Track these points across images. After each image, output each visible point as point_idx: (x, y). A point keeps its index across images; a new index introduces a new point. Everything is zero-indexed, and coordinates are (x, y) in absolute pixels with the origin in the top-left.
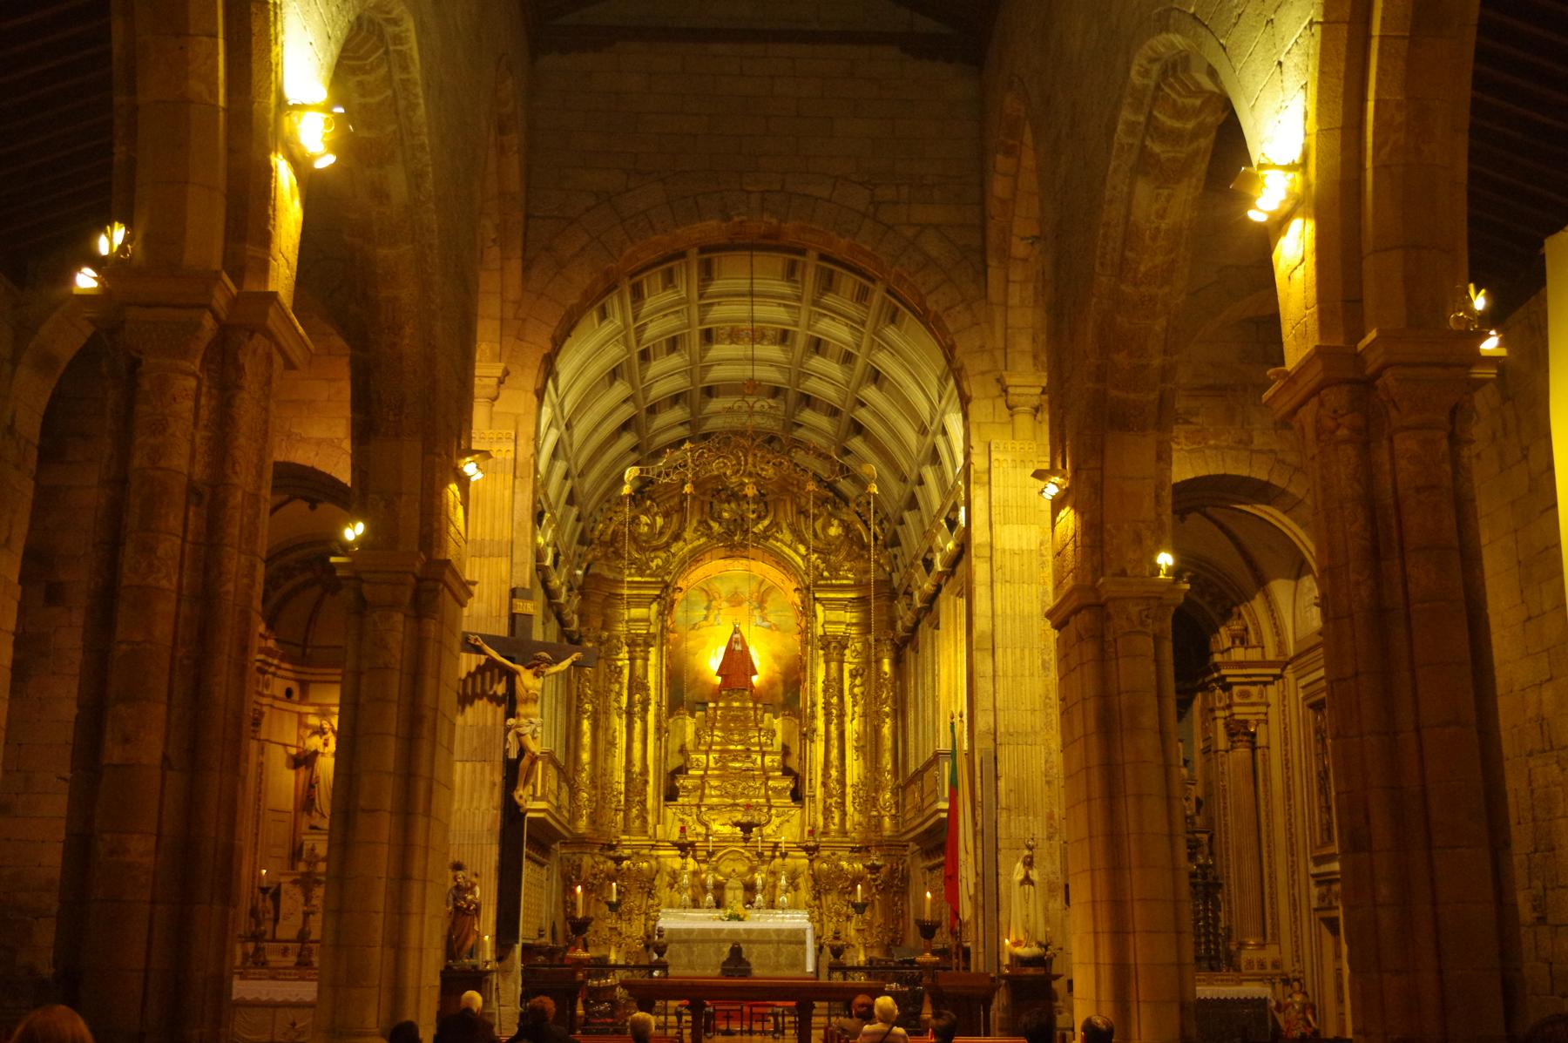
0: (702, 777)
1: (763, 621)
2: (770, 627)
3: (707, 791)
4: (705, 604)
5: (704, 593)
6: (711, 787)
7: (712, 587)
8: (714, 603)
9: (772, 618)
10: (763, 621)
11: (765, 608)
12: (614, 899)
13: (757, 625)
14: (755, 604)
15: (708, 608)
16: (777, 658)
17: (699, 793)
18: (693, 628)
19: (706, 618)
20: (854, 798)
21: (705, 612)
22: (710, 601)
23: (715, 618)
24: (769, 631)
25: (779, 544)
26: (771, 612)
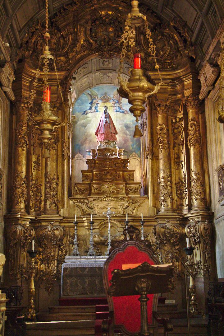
0: (89, 184)
2: (123, 112)
3: (93, 191)
4: (90, 101)
5: (89, 96)
6: (95, 189)
7: (93, 92)
8: (94, 101)
10: (120, 108)
11: (121, 103)
13: (117, 111)
15: (91, 103)
17: (88, 192)
18: (84, 114)
19: (90, 108)
20: (177, 191)
21: (90, 105)
22: (92, 100)
23: (96, 108)
24: (123, 114)
26: (124, 105)
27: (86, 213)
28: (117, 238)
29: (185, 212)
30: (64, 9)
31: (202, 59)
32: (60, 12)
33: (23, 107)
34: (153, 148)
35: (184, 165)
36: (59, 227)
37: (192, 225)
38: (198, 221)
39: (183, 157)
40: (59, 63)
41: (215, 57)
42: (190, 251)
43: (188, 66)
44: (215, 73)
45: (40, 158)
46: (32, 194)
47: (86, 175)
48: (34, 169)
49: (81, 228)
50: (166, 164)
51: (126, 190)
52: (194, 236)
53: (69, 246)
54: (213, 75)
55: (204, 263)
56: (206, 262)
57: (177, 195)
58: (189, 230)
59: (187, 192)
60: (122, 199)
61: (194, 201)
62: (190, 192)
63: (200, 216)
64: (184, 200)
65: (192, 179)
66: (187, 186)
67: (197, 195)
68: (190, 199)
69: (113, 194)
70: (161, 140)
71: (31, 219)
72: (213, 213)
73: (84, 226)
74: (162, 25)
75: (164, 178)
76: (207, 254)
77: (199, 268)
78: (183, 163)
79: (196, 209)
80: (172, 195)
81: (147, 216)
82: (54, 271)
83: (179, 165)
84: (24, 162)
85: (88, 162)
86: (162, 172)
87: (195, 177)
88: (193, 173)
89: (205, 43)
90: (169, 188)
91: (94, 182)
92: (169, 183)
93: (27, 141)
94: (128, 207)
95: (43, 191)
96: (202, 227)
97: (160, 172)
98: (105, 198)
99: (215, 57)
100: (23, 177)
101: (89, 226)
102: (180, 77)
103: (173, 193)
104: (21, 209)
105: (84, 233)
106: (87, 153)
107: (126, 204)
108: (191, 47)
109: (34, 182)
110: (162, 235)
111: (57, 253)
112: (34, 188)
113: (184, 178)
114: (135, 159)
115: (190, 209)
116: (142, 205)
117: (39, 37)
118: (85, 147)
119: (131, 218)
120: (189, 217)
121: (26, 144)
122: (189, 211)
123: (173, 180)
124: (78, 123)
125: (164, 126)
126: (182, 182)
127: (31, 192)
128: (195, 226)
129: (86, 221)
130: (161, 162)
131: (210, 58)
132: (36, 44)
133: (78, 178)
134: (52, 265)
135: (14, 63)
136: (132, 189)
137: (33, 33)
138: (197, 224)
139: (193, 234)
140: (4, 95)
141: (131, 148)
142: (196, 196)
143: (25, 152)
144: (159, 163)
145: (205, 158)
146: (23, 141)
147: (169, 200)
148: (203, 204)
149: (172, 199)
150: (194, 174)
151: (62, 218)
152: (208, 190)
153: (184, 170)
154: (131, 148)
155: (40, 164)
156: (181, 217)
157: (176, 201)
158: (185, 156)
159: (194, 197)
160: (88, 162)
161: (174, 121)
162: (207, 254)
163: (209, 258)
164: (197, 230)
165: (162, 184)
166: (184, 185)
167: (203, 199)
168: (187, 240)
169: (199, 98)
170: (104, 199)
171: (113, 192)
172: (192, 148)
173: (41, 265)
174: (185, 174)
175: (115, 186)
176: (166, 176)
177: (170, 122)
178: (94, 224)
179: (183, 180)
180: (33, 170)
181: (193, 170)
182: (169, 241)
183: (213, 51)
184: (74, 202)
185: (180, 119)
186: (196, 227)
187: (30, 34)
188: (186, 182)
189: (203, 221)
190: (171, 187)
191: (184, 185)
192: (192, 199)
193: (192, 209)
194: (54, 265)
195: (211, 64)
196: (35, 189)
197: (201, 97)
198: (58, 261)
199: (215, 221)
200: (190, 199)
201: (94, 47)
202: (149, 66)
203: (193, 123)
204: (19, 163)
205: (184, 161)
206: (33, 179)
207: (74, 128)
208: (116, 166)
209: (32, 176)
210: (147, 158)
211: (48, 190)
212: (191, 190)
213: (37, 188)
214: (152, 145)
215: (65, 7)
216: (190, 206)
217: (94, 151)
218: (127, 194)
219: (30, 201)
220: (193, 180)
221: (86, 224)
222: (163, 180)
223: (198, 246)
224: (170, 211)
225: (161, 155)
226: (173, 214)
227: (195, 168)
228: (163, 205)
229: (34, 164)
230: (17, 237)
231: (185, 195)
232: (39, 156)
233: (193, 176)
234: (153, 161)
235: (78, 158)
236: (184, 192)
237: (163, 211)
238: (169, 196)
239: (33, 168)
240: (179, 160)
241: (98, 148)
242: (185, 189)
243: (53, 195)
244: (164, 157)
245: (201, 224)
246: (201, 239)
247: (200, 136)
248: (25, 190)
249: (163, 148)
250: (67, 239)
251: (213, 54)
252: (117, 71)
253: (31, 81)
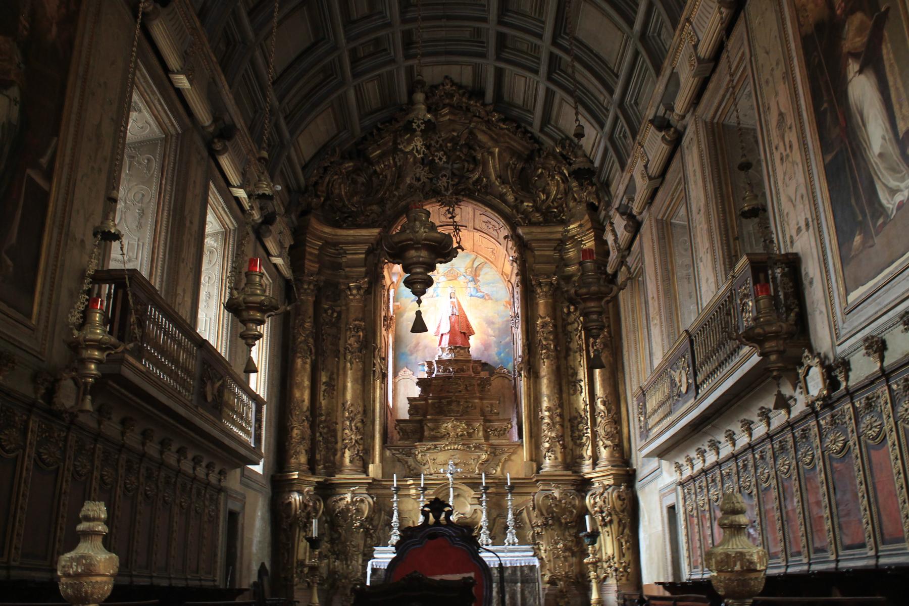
0: (420, 422)
1: (477, 291)
2: (483, 297)
3: (426, 433)
9: (485, 289)
10: (477, 290)
11: (479, 281)
12: (315, 534)
13: (471, 296)
14: (470, 278)
16: (490, 323)
24: (481, 300)
25: (488, 197)
27: (415, 471)
28: (468, 516)
29: (587, 469)
30: (379, 129)
31: (608, 205)
32: (371, 134)
33: (305, 290)
34: (529, 357)
35: (583, 387)
36: (366, 496)
37: (597, 493)
38: (608, 485)
39: (582, 373)
40: (369, 216)
41: (628, 203)
42: (594, 536)
43: (587, 217)
44: (629, 229)
45: (335, 376)
46: (321, 439)
47: (416, 405)
48: (324, 395)
49: (406, 499)
50: (552, 385)
51: (485, 431)
52: (602, 512)
53: (384, 530)
54: (625, 232)
55: (620, 559)
56: (624, 555)
57: (572, 440)
58: (592, 501)
59: (589, 435)
60: (478, 447)
61: (602, 449)
62: (595, 434)
63: (612, 476)
64: (585, 447)
66: (589, 424)
67: (607, 439)
68: (595, 446)
69: (462, 439)
70: (544, 343)
71: (317, 482)
72: (635, 471)
73: (409, 496)
74: (541, 152)
75: (549, 409)
76: (624, 543)
77: (611, 567)
78: (582, 384)
79: (606, 463)
80: (563, 440)
81: (520, 477)
82: (358, 572)
83: (575, 386)
84: (307, 383)
85: (421, 382)
86: (545, 399)
88: (599, 400)
89: (613, 180)
90: (558, 426)
91: (429, 417)
92: (558, 419)
93: (312, 347)
94: (487, 461)
95: (339, 434)
96: (615, 494)
97: (543, 400)
98: (447, 445)
99: (628, 203)
100: (305, 409)
101: (417, 495)
102: (574, 236)
103: (566, 436)
104: (300, 464)
105: (410, 507)
106: (420, 368)
107: (484, 457)
108: (590, 188)
109: (323, 418)
110: (547, 511)
111: (362, 543)
112: (324, 428)
113: (585, 410)
114: (503, 377)
115: (595, 464)
116: (513, 457)
117: (336, 174)
118: (416, 358)
119: (491, 481)
120: (592, 478)
121: (311, 351)
122: (594, 468)
123: (565, 414)
124: (405, 317)
125: (548, 319)
126: (581, 416)
127: (318, 434)
128: (602, 494)
129: (413, 486)
130: (545, 382)
131: (620, 204)
132: (330, 185)
133: (403, 412)
134: (354, 562)
135: (293, 217)
136: (496, 429)
137: (326, 169)
138: (607, 489)
139: (601, 507)
140: (274, 269)
141: (497, 358)
142: (606, 442)
143: (308, 367)
144: (540, 384)
145: (620, 375)
146: (306, 348)
147: (558, 449)
148: (617, 455)
149: (564, 447)
150: (601, 402)
151: (370, 481)
152: (625, 430)
153: (584, 396)
154: (497, 358)
155: (335, 388)
156: (580, 478)
157: (572, 450)
158: (586, 370)
159: (601, 443)
160: (421, 382)
161: (565, 310)
162: (624, 543)
163: (628, 549)
164: (607, 500)
165: (547, 420)
166: (584, 421)
167: (617, 446)
168: (587, 517)
169: (606, 271)
170: (444, 447)
171: (462, 435)
173: (335, 562)
174: (585, 402)
175: (466, 425)
176: (552, 406)
177: (559, 314)
178: (426, 492)
179: (582, 413)
180: (322, 398)
181: (598, 395)
182: (559, 520)
183: (625, 193)
184: (394, 452)
186: (605, 495)
187: (321, 171)
188: (589, 416)
189: (617, 485)
190: (562, 426)
191: (584, 421)
192: (598, 446)
193: (597, 465)
194: (357, 561)
195: (622, 214)
196: (325, 430)
197: (610, 270)
198: (364, 555)
199: (638, 485)
200: (595, 446)
201: (427, 189)
202: (521, 218)
204: (300, 386)
205: (583, 379)
206: (323, 412)
207: (397, 325)
208: (468, 391)
209: (321, 407)
210: (520, 375)
211: (347, 431)
212: (597, 431)
213: (328, 427)
214: (529, 353)
215: (380, 126)
217: (430, 364)
218: (487, 438)
219: (317, 451)
220: (599, 413)
221: (413, 491)
222: (547, 413)
223: (608, 529)
224: (559, 468)
225: (545, 369)
226: (565, 473)
227: (602, 392)
228: (547, 458)
229: (323, 388)
230: (293, 512)
231: (587, 440)
232: (332, 374)
233: (600, 406)
234: (530, 380)
235: (405, 377)
236: (584, 434)
237: (548, 469)
238: (559, 441)
239: (322, 393)
240: (576, 379)
241: (437, 359)
242: (587, 429)
243: (356, 441)
244: (548, 374)
245: (613, 490)
246: (615, 517)
247: (610, 337)
248: (309, 432)
249: (547, 358)
250: (380, 517)
251: (625, 198)
252: (469, 228)
253: (322, 246)
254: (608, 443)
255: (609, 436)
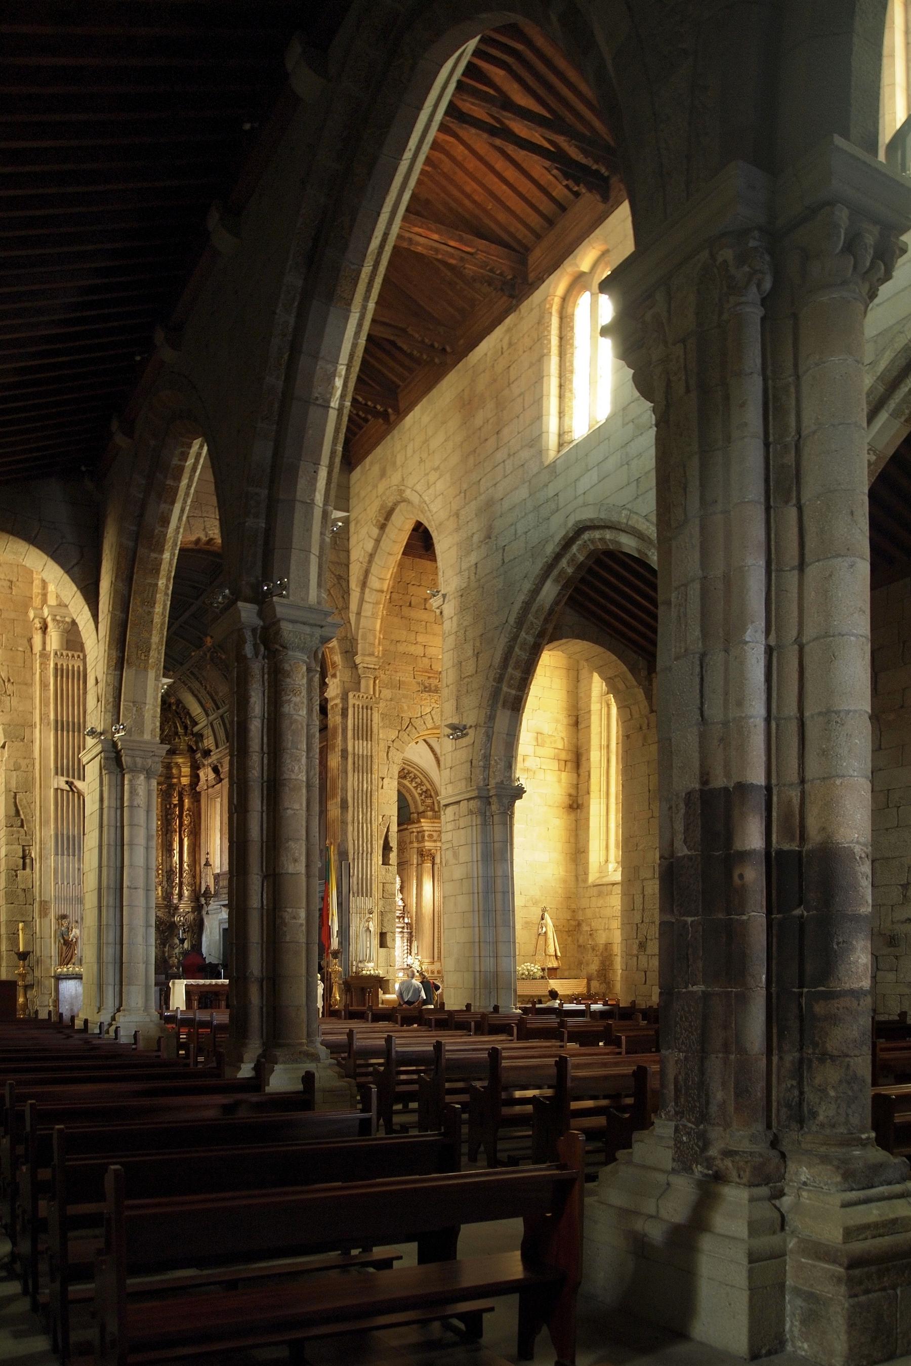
61: (185, 891)
65: (184, 870)
87: (187, 868)
149: (163, 887)
153: (176, 858)
172: (186, 839)
185: (175, 805)
189: (193, 912)
203: (189, 814)
216: (181, 895)
233: (185, 866)
254: (189, 888)
255: (189, 884)
